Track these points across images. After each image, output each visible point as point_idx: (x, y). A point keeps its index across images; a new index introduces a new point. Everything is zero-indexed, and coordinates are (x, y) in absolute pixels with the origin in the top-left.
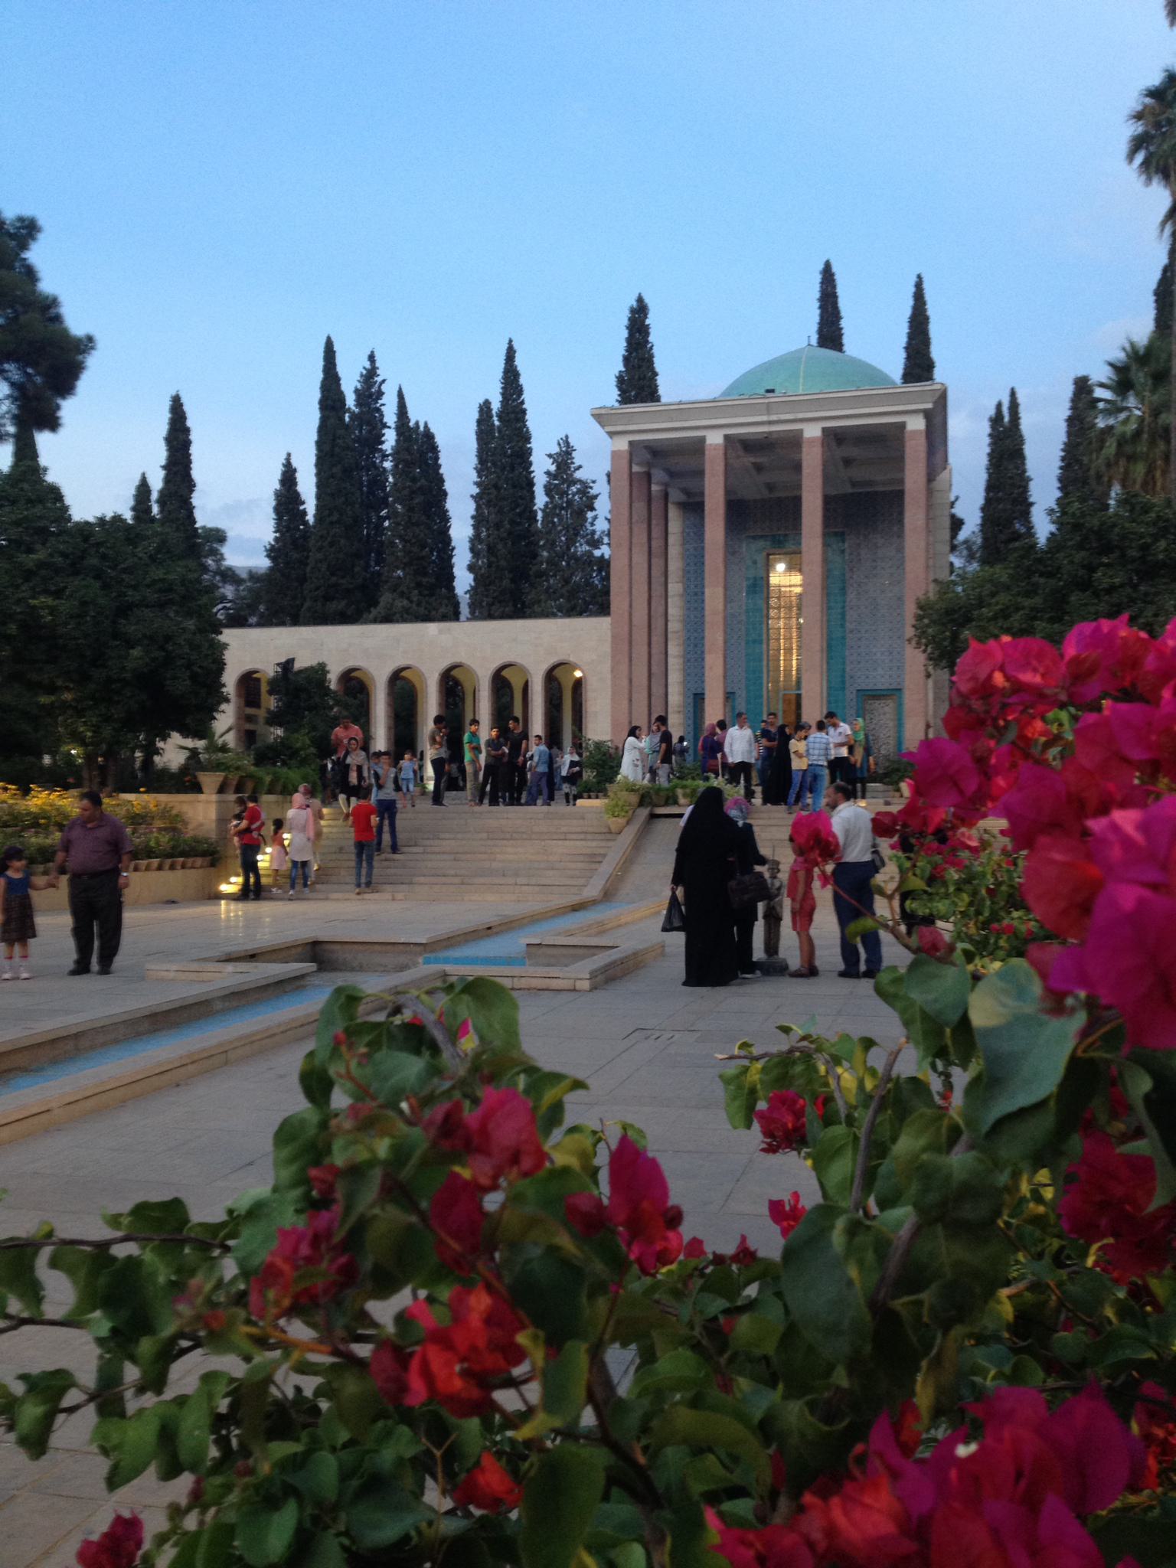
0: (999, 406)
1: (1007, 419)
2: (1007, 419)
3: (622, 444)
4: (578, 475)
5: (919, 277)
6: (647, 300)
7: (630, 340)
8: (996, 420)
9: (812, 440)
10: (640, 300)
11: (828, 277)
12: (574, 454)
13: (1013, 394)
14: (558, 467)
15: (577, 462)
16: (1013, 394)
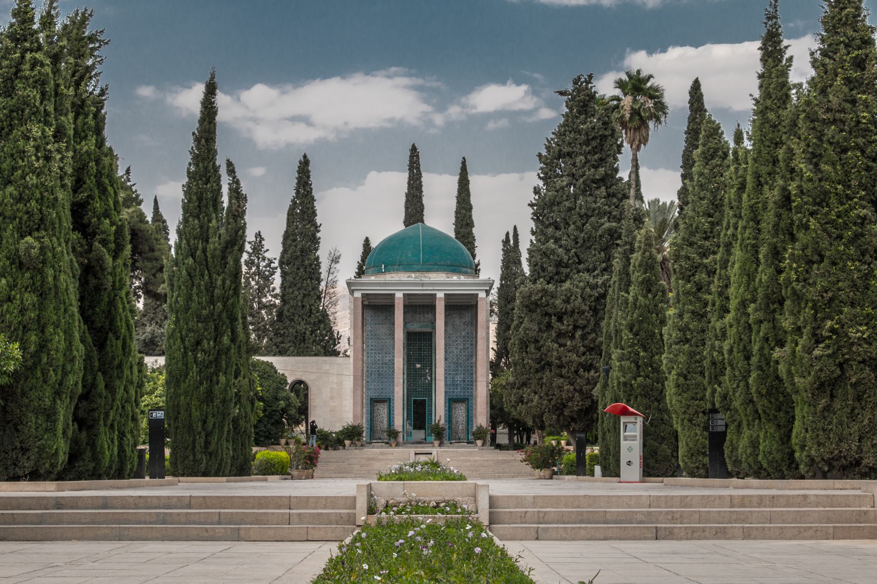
0: (508, 234)
1: (512, 242)
2: (512, 242)
3: (358, 295)
4: (267, 255)
5: (464, 158)
6: (309, 157)
7: (299, 179)
8: (506, 242)
9: (440, 298)
10: (305, 156)
11: (414, 149)
12: (263, 242)
13: (515, 228)
14: (254, 249)
15: (265, 248)
16: (515, 228)
